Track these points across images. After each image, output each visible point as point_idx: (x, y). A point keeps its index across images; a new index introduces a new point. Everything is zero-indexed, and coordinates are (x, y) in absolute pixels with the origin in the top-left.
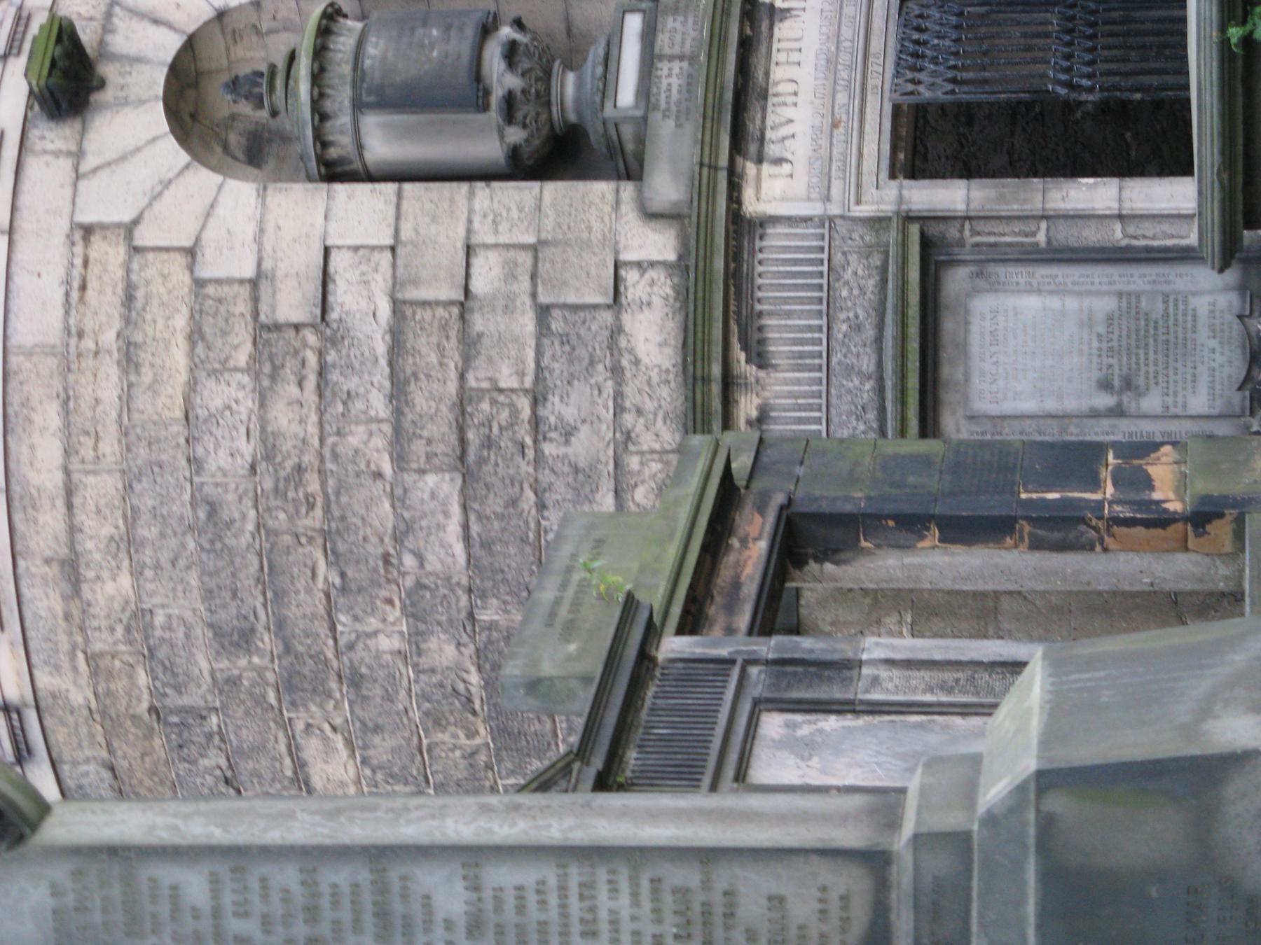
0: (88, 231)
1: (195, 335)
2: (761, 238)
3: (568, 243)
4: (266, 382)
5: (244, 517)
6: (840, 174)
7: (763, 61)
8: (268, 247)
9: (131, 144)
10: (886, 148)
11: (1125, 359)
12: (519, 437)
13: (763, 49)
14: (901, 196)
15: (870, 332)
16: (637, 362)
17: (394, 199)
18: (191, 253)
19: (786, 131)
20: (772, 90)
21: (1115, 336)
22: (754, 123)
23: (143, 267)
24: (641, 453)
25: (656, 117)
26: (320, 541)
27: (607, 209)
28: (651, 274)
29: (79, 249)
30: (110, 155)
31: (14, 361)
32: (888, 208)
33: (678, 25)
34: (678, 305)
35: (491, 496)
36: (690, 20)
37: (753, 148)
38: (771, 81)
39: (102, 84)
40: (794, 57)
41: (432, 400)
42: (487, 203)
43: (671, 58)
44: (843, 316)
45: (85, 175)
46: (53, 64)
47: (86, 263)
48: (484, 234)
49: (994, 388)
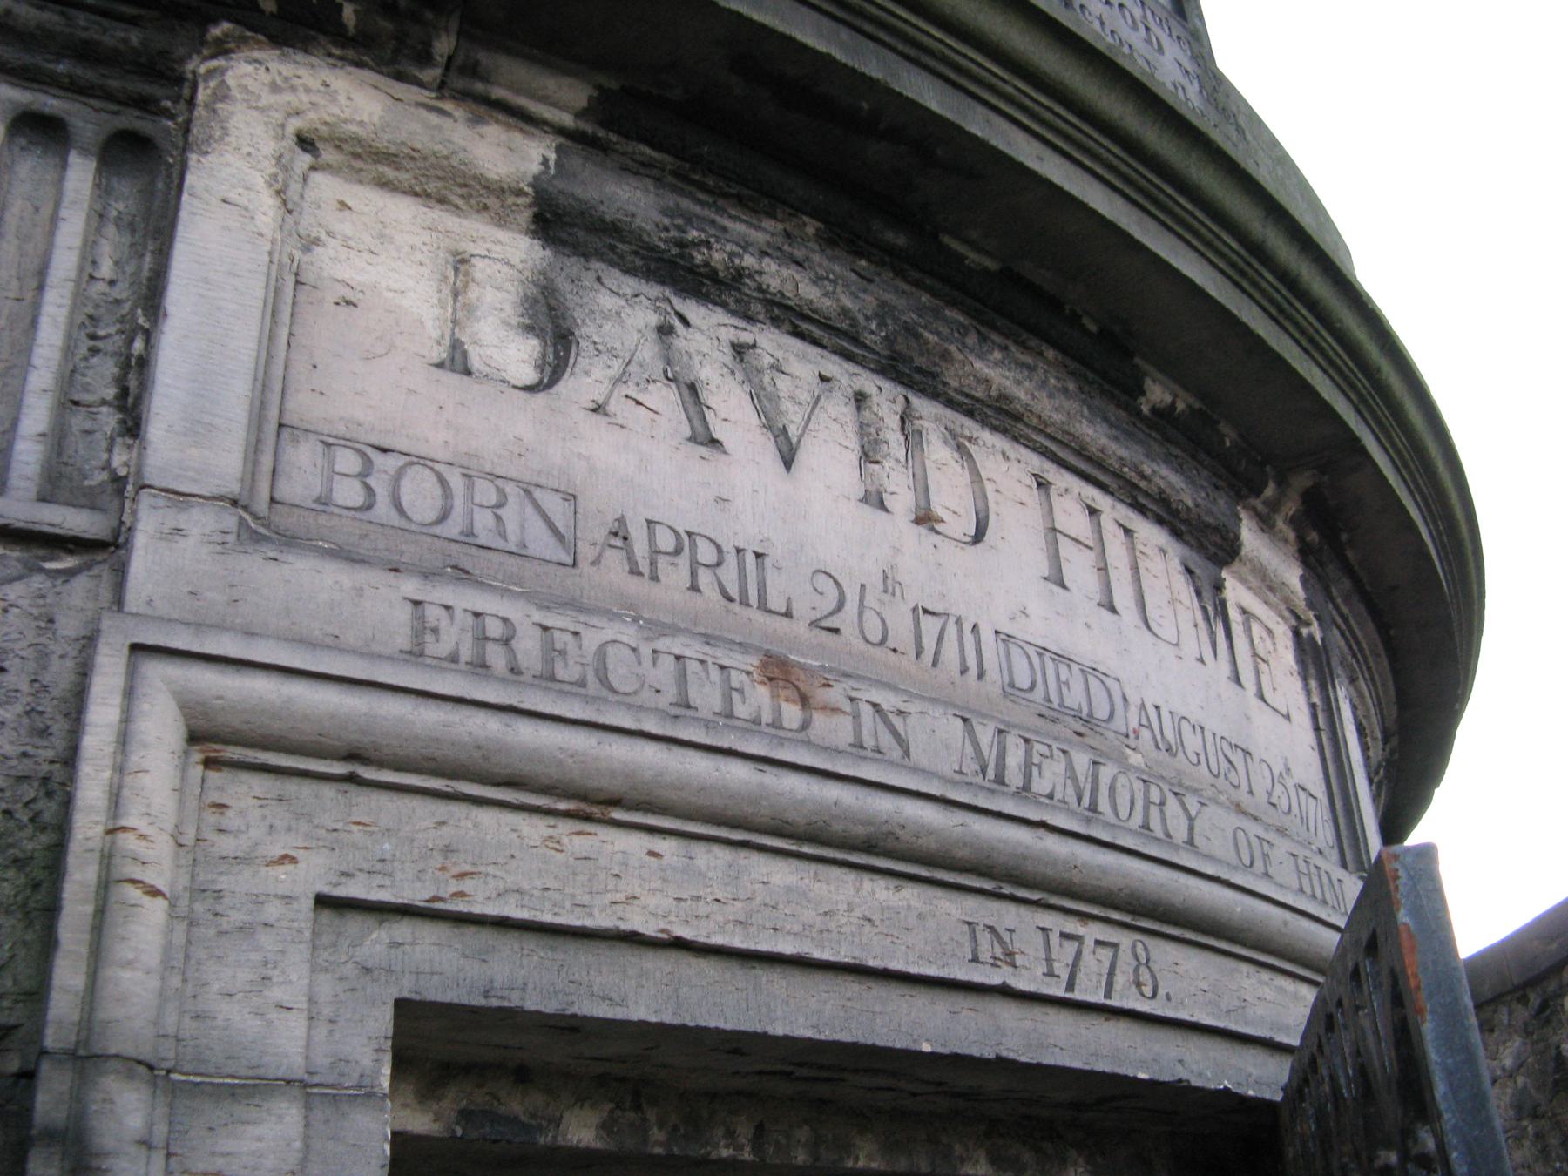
10: (641, 995)
14: (252, 1088)
37: (633, 200)
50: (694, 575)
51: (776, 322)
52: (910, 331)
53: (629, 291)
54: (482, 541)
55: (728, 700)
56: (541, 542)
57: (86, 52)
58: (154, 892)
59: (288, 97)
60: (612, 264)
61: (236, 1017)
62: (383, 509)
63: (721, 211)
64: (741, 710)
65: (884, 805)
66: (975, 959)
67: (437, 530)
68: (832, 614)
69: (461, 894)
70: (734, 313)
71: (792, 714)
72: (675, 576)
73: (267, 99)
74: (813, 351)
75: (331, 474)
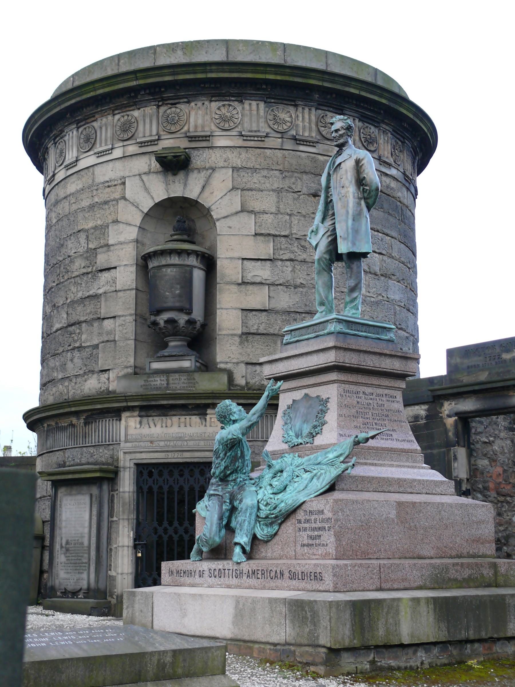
0: (124, 183)
1: (95, 228)
2: (116, 420)
3: (115, 352)
4: (85, 255)
5: (61, 256)
6: (134, 445)
8: (116, 247)
9: (152, 190)
11: (73, 549)
12: (72, 344)
13: (184, 413)
15: (91, 460)
16: (86, 381)
17: (130, 288)
18: (116, 222)
19: (152, 424)
21: (79, 546)
23: (114, 205)
24: (68, 386)
25: (145, 377)
26: (58, 282)
27: (125, 364)
28: (106, 381)
29: (120, 182)
30: (147, 184)
31: (91, 169)
32: (121, 464)
33: (183, 380)
34: (99, 392)
35: (61, 337)
36: (185, 385)
37: (143, 413)
39: (175, 174)
40: (182, 425)
41: (81, 313)
42: (128, 321)
43: (168, 380)
44: (95, 451)
45: (141, 177)
46: (165, 157)
47: (115, 185)
48: (119, 321)
49: (68, 505)
56: (140, 437)
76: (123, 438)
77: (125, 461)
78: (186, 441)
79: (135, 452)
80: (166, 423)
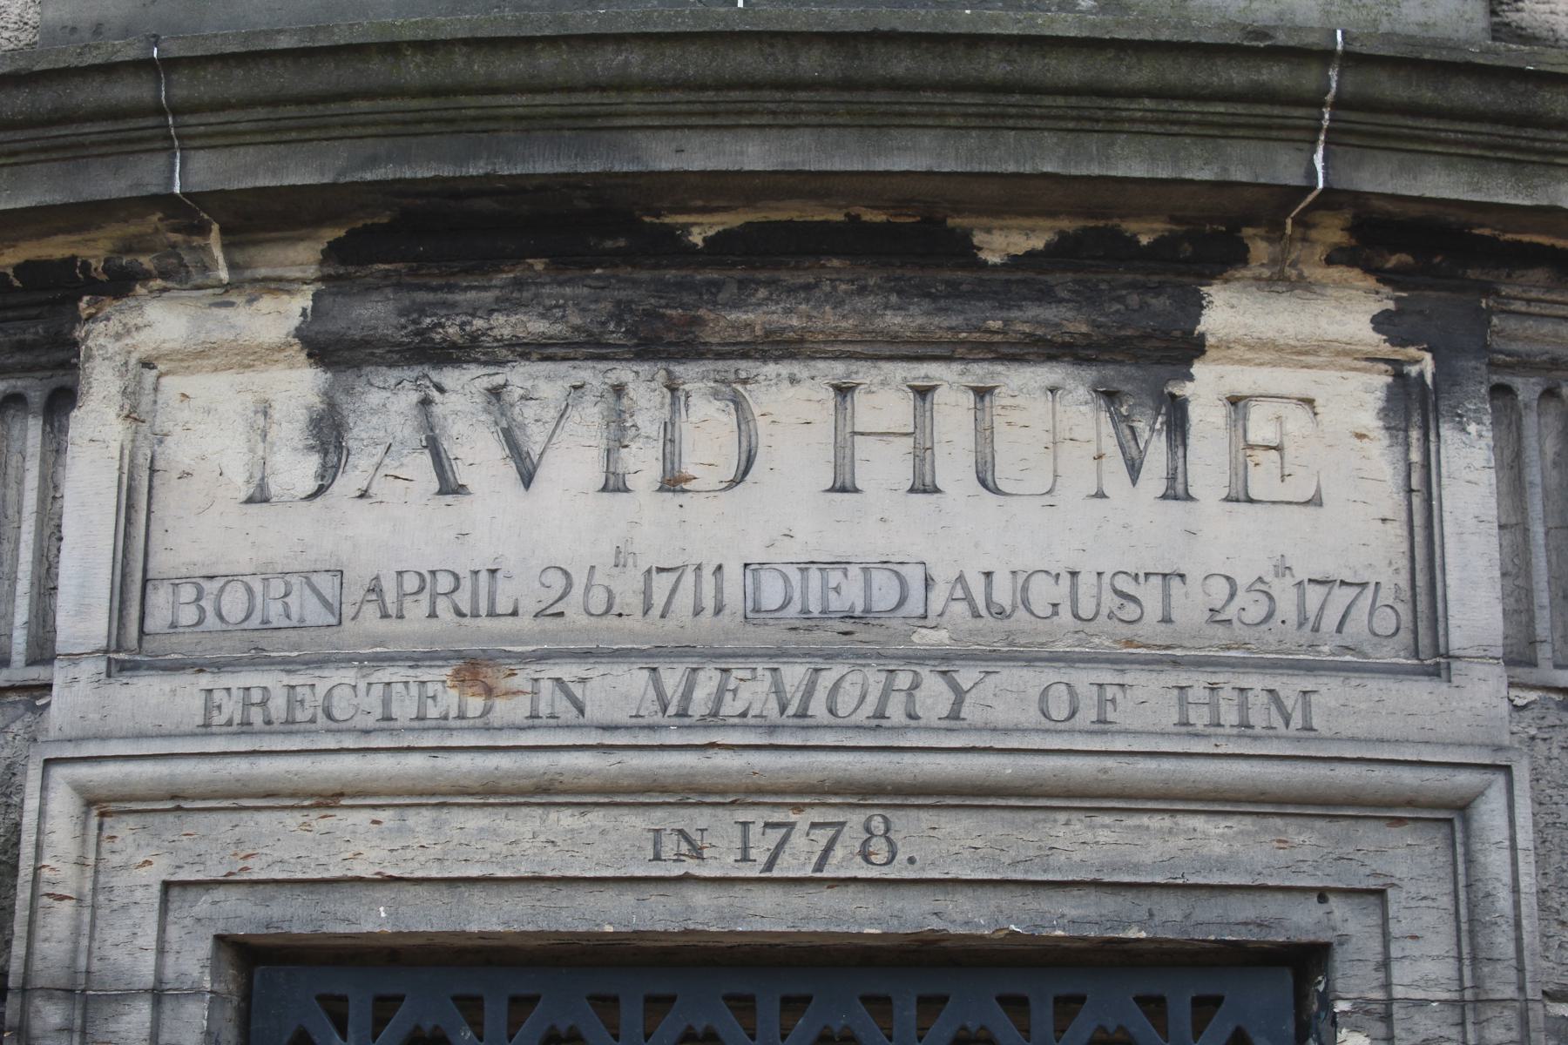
6: (231, 709)
7: (829, 319)
14: (126, 996)
19: (478, 452)
20: (690, 373)
22: (506, 305)
37: (375, 313)
38: (746, 367)
40: (882, 467)
50: (433, 604)
51: (525, 356)
52: (651, 314)
53: (393, 382)
54: (274, 625)
55: (421, 705)
56: (315, 613)
57: (22, 346)
58: (62, 898)
59: (128, 341)
60: (378, 364)
61: (120, 957)
62: (211, 621)
63: (451, 288)
64: (433, 712)
65: (540, 762)
66: (657, 858)
67: (245, 625)
68: (561, 598)
69: (246, 869)
70: (486, 364)
71: (475, 705)
72: (417, 610)
73: (113, 347)
74: (564, 367)
75: (175, 605)
76: (83, 618)
77: (93, 903)
78: (944, 661)
79: (239, 798)
80: (670, 440)
